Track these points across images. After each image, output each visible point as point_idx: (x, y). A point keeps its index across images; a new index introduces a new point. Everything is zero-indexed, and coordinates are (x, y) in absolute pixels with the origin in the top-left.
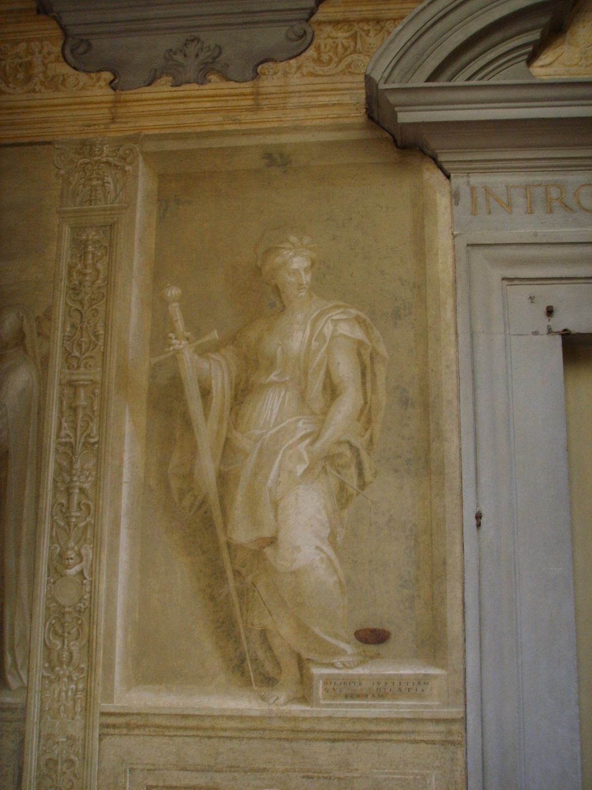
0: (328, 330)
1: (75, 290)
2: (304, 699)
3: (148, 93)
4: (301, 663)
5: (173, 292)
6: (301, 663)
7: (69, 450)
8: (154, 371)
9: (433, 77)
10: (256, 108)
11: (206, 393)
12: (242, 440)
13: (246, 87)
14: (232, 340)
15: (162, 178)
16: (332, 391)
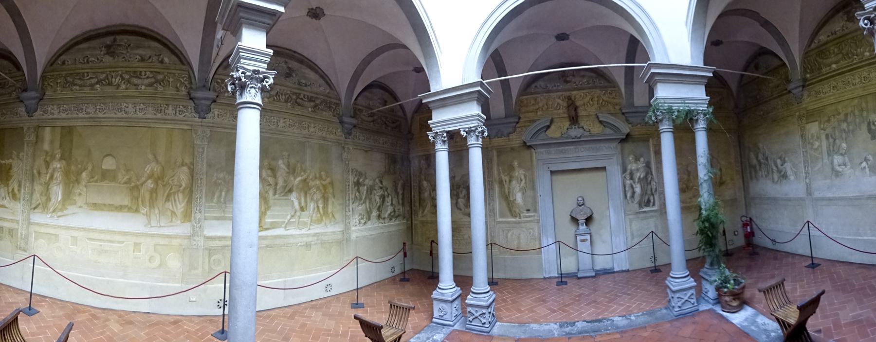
0: (520, 172)
1: (488, 169)
2: (520, 218)
3: (495, 139)
4: (520, 214)
5: (500, 168)
6: (520, 214)
7: (489, 189)
8: (499, 178)
9: (530, 139)
10: (509, 141)
11: (506, 181)
12: (511, 187)
13: (507, 138)
14: (509, 174)
15: (497, 152)
16: (521, 180)
